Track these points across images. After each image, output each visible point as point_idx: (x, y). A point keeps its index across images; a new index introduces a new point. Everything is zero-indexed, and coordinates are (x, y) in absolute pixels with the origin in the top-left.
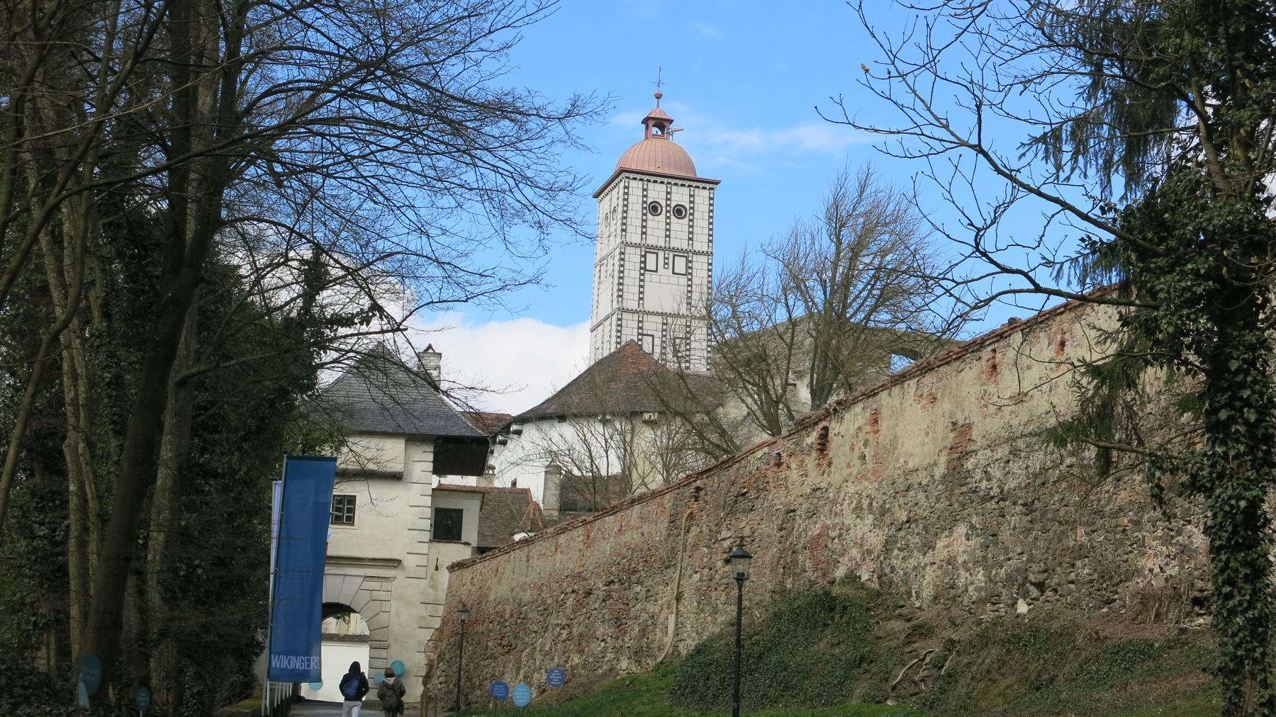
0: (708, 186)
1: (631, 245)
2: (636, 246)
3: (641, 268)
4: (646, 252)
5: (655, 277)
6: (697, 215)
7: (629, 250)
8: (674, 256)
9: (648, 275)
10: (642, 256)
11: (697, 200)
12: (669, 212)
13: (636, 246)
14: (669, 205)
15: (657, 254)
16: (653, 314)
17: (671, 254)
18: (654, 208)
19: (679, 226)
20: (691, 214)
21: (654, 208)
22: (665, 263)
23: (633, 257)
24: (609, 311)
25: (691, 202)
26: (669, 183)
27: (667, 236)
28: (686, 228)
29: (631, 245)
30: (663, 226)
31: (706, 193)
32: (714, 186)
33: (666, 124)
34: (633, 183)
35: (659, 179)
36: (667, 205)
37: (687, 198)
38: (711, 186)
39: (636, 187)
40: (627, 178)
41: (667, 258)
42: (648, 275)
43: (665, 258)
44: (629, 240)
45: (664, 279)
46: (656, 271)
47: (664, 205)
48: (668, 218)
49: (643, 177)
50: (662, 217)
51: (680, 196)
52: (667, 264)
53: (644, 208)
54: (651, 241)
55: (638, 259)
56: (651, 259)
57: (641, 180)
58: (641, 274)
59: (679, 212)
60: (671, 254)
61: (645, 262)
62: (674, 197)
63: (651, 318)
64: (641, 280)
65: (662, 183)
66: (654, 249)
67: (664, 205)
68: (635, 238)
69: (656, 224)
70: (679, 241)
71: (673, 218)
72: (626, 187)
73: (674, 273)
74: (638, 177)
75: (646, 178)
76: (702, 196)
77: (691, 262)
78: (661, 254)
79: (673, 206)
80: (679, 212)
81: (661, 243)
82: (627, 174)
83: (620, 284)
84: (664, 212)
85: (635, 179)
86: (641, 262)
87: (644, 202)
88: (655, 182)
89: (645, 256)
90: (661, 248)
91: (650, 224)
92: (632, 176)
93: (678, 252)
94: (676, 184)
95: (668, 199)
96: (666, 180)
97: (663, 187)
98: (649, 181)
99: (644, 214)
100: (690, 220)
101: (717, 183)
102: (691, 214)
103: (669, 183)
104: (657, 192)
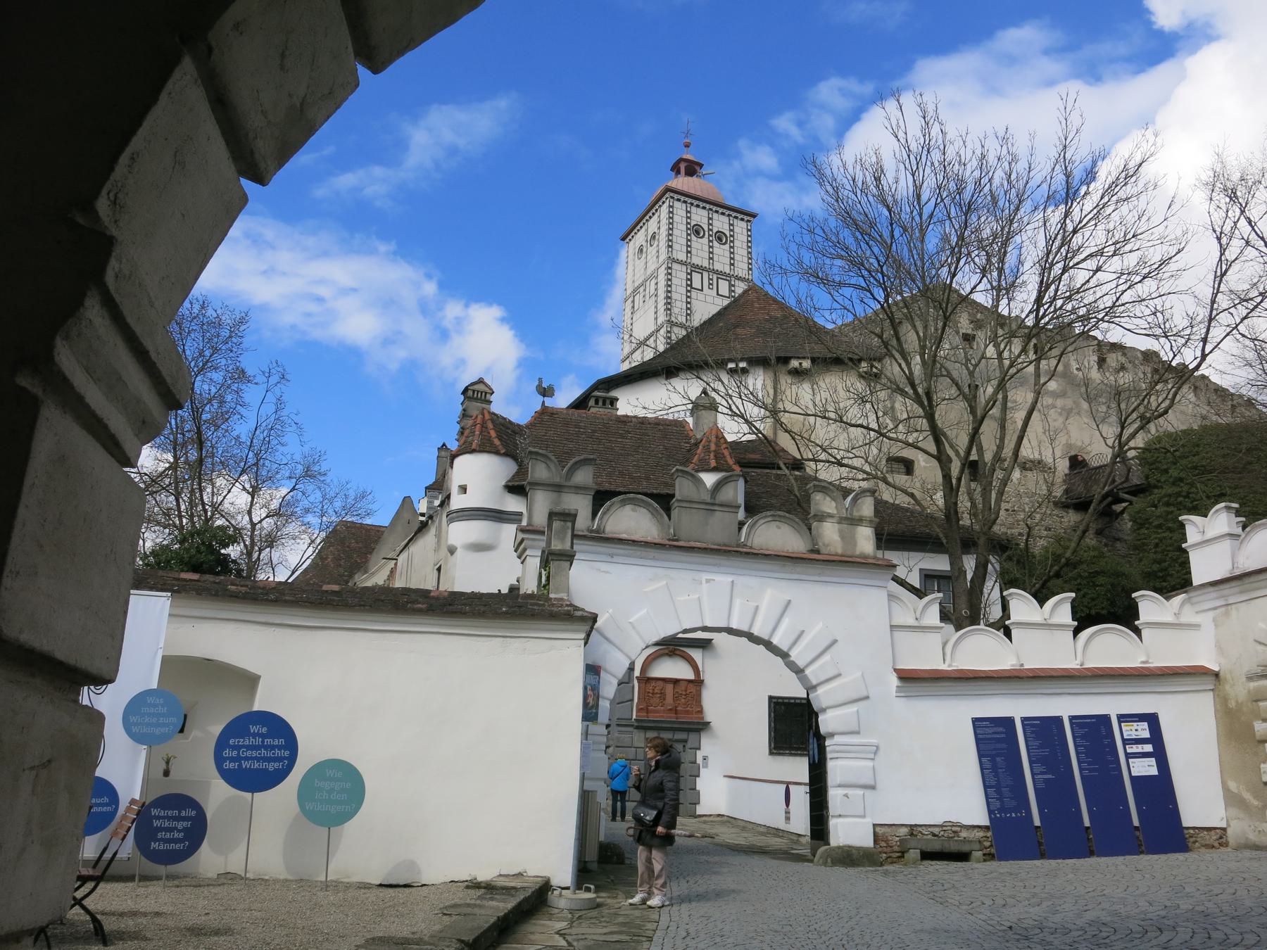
0: (746, 218)
1: (678, 262)
2: (681, 263)
3: (687, 285)
4: (692, 271)
5: (701, 296)
6: (737, 243)
7: (675, 266)
8: (718, 278)
9: (694, 294)
10: (688, 274)
11: (736, 229)
12: (711, 236)
13: (681, 263)
14: (712, 230)
15: (702, 274)
17: (715, 276)
18: (696, 231)
19: (721, 251)
20: (731, 241)
21: (696, 231)
22: (710, 284)
23: (680, 274)
24: (653, 328)
25: (731, 230)
26: (711, 209)
27: (710, 258)
28: (727, 254)
29: (678, 262)
30: (706, 248)
31: (743, 224)
32: (752, 219)
33: (697, 168)
34: (677, 204)
35: (702, 204)
36: (709, 230)
37: (727, 227)
38: (749, 218)
39: (680, 209)
40: (672, 198)
41: (712, 280)
42: (694, 294)
43: (709, 279)
44: (675, 256)
45: (709, 299)
46: (702, 290)
47: (706, 229)
48: (710, 241)
49: (686, 199)
50: (705, 240)
51: (721, 223)
52: (712, 284)
53: (687, 229)
54: (696, 261)
55: (684, 276)
56: (696, 278)
57: (685, 202)
58: (688, 291)
59: (720, 237)
60: (715, 276)
61: (691, 280)
62: (715, 223)
64: (688, 297)
66: (700, 269)
67: (706, 229)
68: (682, 256)
69: (700, 245)
70: (722, 264)
71: (715, 242)
72: (670, 206)
73: (718, 294)
74: (683, 198)
75: (689, 200)
76: (740, 227)
77: (734, 286)
78: (705, 275)
79: (714, 231)
80: (720, 237)
81: (705, 264)
82: (672, 194)
83: (668, 297)
84: (707, 233)
85: (679, 200)
86: (687, 279)
87: (688, 223)
88: (698, 206)
89: (691, 275)
90: (704, 269)
91: (694, 244)
92: (676, 196)
93: (721, 275)
94: (717, 212)
95: (709, 224)
96: (708, 206)
97: (705, 213)
98: (692, 204)
99: (688, 234)
100: (731, 247)
101: (754, 216)
102: (731, 241)
103: (711, 209)
104: (699, 216)
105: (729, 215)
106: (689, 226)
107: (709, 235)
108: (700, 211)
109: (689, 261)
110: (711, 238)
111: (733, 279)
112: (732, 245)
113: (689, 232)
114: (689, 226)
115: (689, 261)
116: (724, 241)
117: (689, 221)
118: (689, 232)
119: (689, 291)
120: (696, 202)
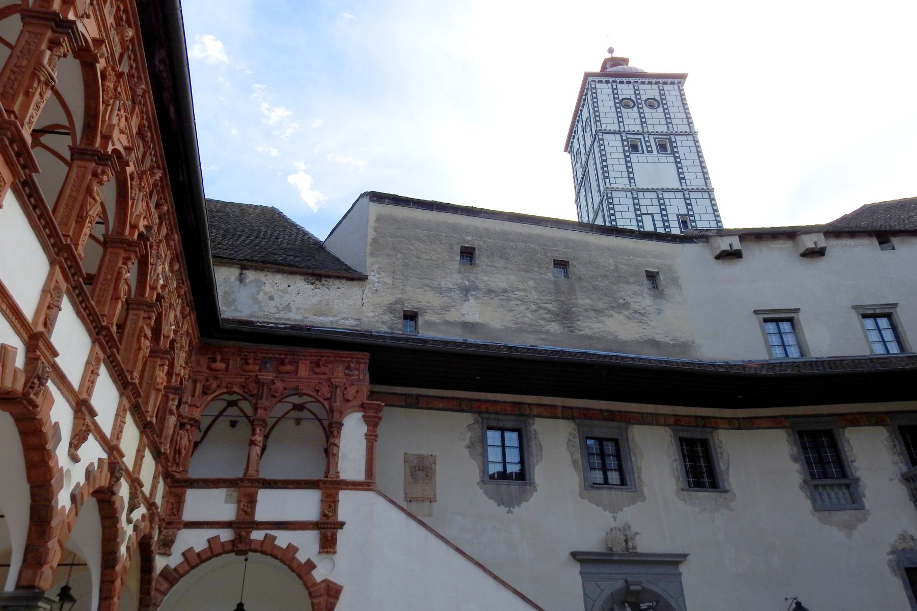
2: (614, 133)
13: (614, 133)
14: (640, 99)
16: (648, 190)
32: (682, 80)
37: (657, 92)
40: (593, 81)
53: (615, 103)
59: (652, 103)
63: (647, 195)
65: (629, 83)
71: (646, 109)
74: (604, 79)
75: (611, 80)
80: (652, 103)
87: (615, 99)
99: (616, 108)
100: (664, 109)
101: (683, 77)
105: (657, 83)
106: (617, 101)
107: (641, 103)
108: (625, 86)
109: (622, 129)
110: (640, 106)
111: (673, 137)
112: (665, 107)
113: (618, 105)
114: (617, 101)
115: (622, 129)
116: (656, 105)
117: (616, 96)
118: (618, 105)
119: (629, 156)
120: (618, 80)
